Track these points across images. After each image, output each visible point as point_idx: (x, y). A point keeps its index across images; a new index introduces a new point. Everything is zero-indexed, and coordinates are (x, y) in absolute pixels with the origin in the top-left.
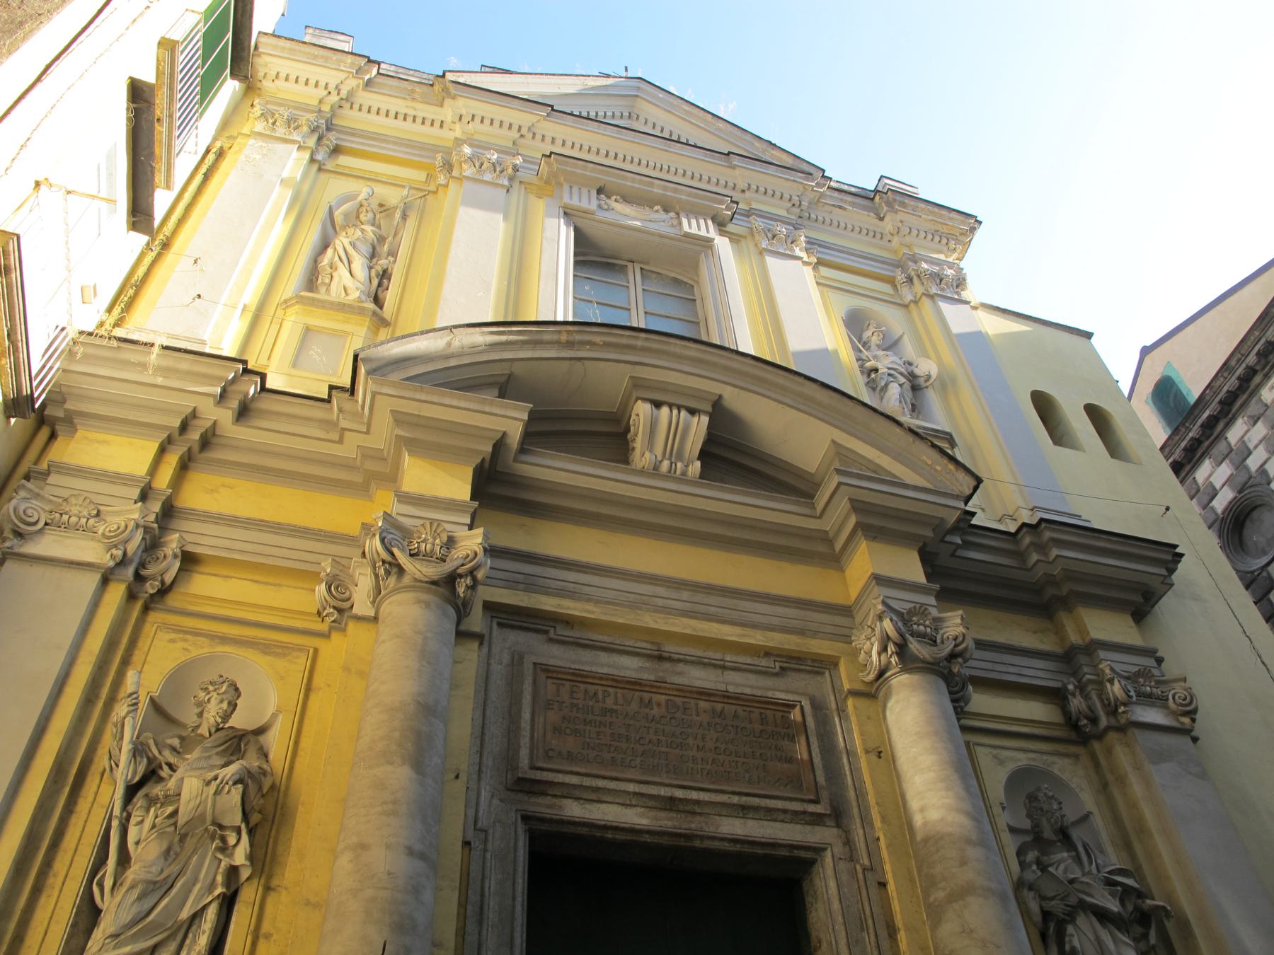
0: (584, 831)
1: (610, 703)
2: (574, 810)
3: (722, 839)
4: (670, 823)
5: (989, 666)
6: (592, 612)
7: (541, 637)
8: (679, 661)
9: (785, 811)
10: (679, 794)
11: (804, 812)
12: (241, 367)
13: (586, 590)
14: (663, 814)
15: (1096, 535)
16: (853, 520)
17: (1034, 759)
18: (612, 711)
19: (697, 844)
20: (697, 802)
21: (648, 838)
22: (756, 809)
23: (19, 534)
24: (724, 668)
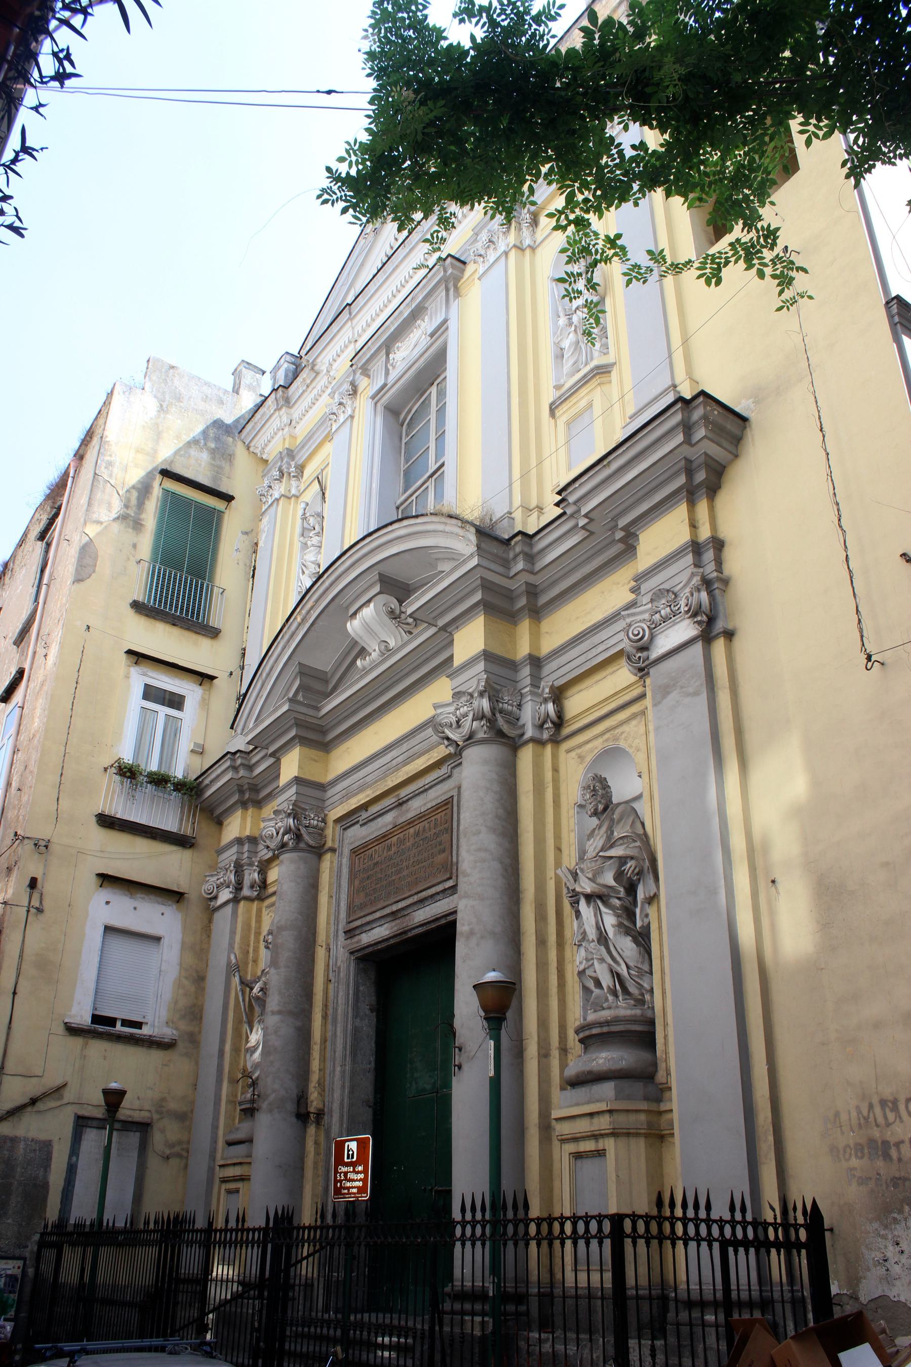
0: (371, 949)
1: (377, 859)
2: (366, 938)
3: (417, 927)
4: (395, 928)
5: (582, 659)
6: (368, 796)
7: (358, 826)
8: (408, 800)
9: (438, 893)
10: (395, 908)
11: (445, 890)
12: (229, 756)
13: (368, 779)
14: (393, 923)
15: (605, 462)
16: (478, 596)
17: (607, 740)
18: (377, 863)
19: (410, 935)
20: (403, 909)
21: (392, 941)
22: (426, 899)
23: (211, 899)
24: (426, 790)
